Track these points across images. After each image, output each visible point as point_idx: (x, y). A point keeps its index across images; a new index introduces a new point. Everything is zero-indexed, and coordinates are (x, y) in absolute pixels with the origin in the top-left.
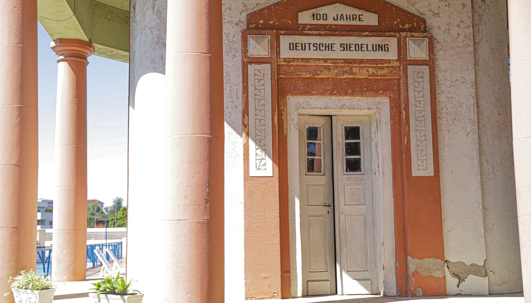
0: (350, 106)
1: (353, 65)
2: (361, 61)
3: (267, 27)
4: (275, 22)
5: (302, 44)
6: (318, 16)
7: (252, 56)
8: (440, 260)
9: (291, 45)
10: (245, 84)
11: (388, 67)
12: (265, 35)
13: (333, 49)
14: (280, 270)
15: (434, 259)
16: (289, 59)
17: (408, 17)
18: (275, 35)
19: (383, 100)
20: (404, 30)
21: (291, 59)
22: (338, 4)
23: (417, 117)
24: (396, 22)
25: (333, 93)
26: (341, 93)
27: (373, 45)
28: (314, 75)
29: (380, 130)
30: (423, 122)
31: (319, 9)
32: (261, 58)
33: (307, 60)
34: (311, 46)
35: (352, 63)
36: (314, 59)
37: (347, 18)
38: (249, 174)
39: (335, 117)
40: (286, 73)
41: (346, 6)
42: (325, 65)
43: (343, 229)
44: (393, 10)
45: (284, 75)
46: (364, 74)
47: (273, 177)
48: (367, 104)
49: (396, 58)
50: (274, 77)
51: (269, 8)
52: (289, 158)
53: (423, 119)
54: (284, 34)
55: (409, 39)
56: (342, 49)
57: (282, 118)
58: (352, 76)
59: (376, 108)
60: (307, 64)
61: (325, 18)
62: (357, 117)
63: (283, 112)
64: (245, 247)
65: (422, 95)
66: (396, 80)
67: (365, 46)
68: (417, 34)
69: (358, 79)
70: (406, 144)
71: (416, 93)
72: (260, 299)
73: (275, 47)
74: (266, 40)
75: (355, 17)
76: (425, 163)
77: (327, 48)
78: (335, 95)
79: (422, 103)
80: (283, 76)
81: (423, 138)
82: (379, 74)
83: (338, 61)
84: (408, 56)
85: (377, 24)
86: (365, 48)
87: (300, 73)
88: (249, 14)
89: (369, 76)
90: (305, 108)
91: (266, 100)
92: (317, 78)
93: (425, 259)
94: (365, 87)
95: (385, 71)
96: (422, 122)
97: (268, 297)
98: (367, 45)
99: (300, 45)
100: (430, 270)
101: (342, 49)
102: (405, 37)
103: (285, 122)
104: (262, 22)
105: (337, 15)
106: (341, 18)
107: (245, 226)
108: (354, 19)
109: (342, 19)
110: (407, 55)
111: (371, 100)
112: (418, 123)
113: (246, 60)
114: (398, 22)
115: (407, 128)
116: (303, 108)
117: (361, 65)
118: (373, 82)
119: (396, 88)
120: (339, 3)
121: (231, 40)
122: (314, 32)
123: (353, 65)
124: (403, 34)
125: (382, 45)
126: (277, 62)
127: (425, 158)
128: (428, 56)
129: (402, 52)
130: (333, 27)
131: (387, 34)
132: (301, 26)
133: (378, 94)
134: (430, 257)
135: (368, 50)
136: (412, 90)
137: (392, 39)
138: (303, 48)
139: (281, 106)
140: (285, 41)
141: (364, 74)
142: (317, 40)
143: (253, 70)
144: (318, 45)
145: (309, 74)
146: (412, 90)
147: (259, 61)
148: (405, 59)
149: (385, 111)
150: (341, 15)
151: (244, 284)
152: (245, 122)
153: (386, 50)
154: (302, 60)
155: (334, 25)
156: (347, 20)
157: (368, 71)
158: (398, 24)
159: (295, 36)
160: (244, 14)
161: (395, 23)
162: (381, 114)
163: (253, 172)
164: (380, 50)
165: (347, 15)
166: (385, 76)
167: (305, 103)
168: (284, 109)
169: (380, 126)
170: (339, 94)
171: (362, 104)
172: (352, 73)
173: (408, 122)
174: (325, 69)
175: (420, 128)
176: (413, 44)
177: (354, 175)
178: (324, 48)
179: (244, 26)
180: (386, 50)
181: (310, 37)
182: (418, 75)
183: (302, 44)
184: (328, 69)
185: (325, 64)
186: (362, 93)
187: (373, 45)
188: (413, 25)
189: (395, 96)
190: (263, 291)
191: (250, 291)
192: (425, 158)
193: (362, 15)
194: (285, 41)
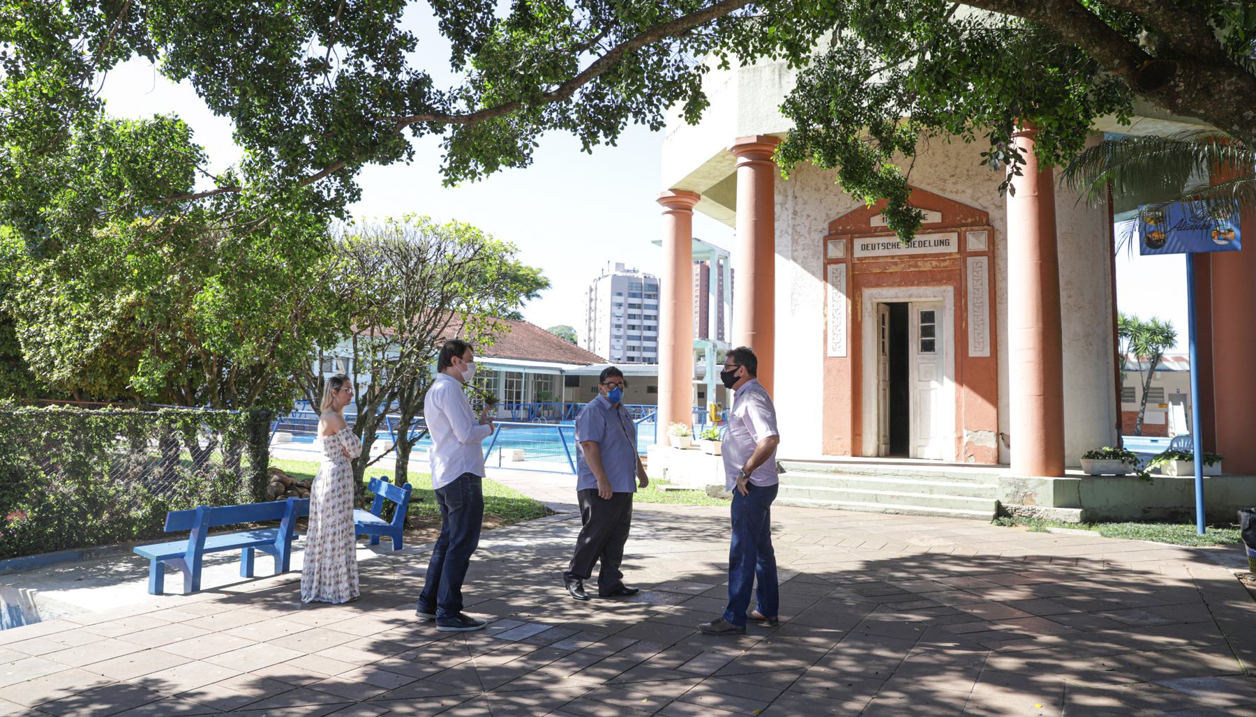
2: (925, 256)
3: (844, 233)
20: (966, 225)
33: (877, 258)
51: (846, 216)
52: (863, 341)
68: (977, 228)
73: (850, 248)
85: (940, 221)
86: (927, 244)
95: (947, 263)
102: (966, 231)
112: (976, 309)
119: (958, 277)
124: (964, 229)
138: (873, 248)
140: (858, 243)
142: (885, 240)
147: (836, 261)
148: (965, 251)
154: (873, 258)
163: (831, 353)
170: (906, 285)
172: (917, 266)
173: (966, 309)
177: (928, 354)
179: (826, 233)
184: (896, 264)
186: (927, 283)
194: (858, 243)
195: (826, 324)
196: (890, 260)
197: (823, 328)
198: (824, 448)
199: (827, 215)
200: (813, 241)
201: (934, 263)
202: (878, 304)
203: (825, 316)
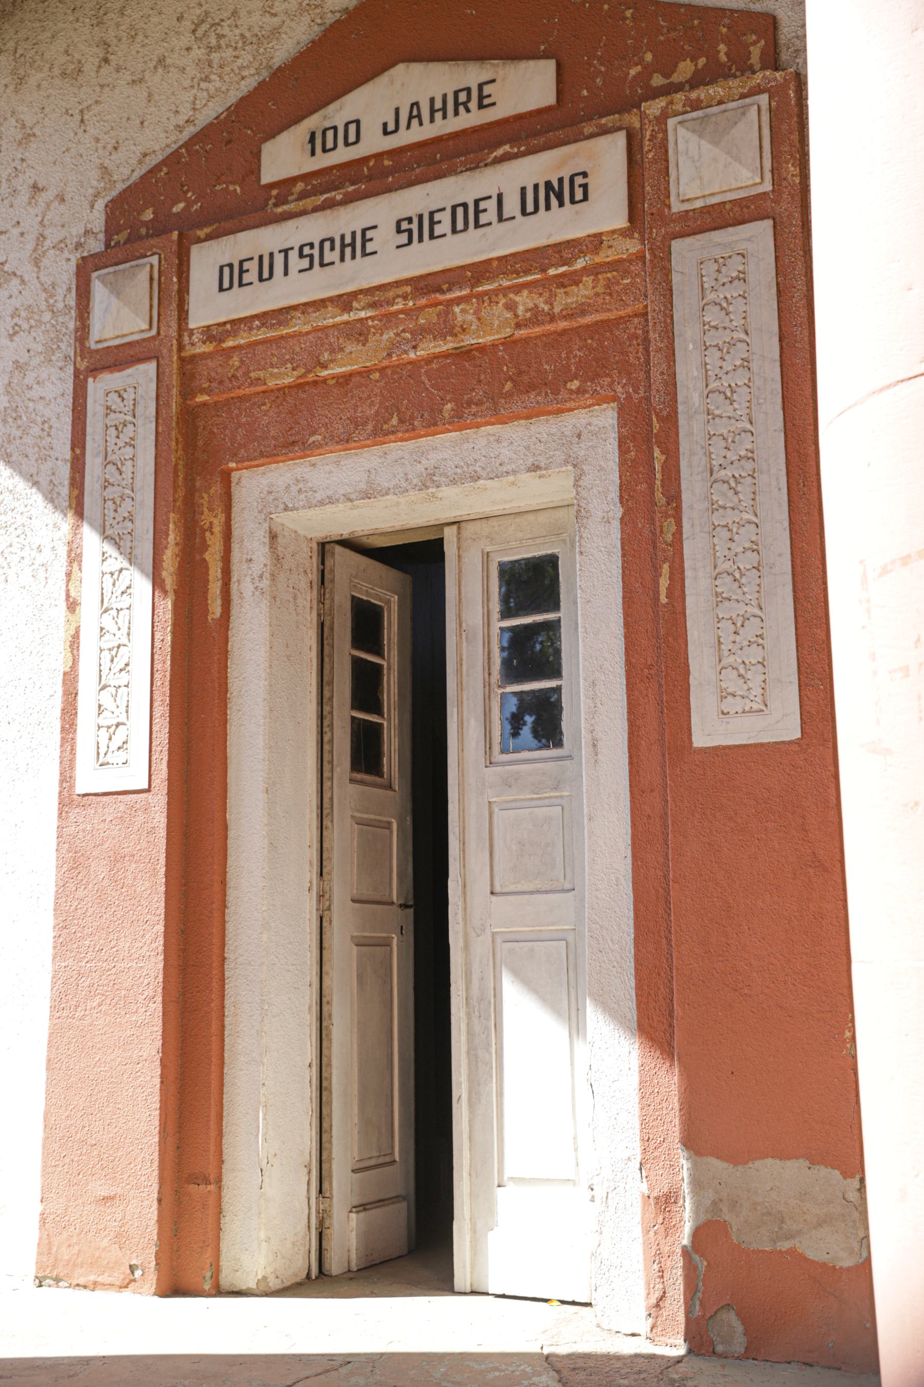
0: (459, 471)
1: (449, 296)
3: (159, 229)
4: (189, 204)
5: (261, 257)
6: (330, 134)
7: (100, 346)
8: (837, 1173)
9: (226, 271)
10: (78, 451)
11: (594, 270)
12: (146, 256)
13: (370, 247)
14: (156, 1173)
15: (803, 1163)
16: (221, 329)
17: (692, 28)
18: (175, 248)
19: (595, 421)
21: (228, 327)
22: (401, 67)
23: (716, 468)
24: (639, 68)
25: (385, 427)
26: (416, 423)
27: (523, 190)
28: (309, 371)
29: (581, 553)
30: (745, 489)
31: (332, 107)
32: (130, 344)
33: (281, 315)
34: (293, 255)
35: (445, 287)
36: (304, 307)
37: (433, 111)
38: (72, 786)
39: (455, 527)
40: (214, 385)
41: (432, 65)
42: (347, 323)
43: (481, 1000)
44: (625, 18)
45: (208, 391)
46: (496, 323)
47: (148, 790)
48: (528, 448)
49: (622, 222)
50: (168, 405)
53: (743, 469)
54: (209, 238)
55: (680, 123)
56: (404, 238)
57: (205, 560)
58: (447, 345)
59: (566, 462)
60: (285, 331)
61: (352, 138)
62: (542, 517)
63: (208, 534)
64: (48, 1069)
65: (738, 363)
66: (636, 320)
67: (491, 206)
68: (716, 90)
69: (482, 349)
70: (663, 599)
71: (713, 357)
72: (85, 1287)
74: (143, 275)
75: (463, 97)
76: (755, 680)
77: (348, 250)
78: (393, 433)
79: (742, 396)
80: (205, 398)
81: (746, 561)
82: (557, 310)
83: (391, 294)
84: (673, 198)
86: (490, 215)
87: (261, 374)
88: (111, 201)
89: (518, 326)
90: (294, 509)
91: (138, 497)
92: (325, 381)
93: (758, 1163)
94: (510, 378)
96: (739, 488)
97: (109, 1280)
98: (500, 197)
99: (253, 266)
100: (783, 1222)
101: (404, 238)
102: (662, 119)
103: (215, 572)
104: (148, 215)
105: (397, 111)
106: (411, 117)
107: (54, 984)
108: (461, 108)
109: (415, 122)
110: (669, 197)
111: (544, 427)
113: (83, 365)
114: (645, 68)
115: (670, 526)
116: (286, 509)
117: (480, 289)
118: (540, 350)
120: (403, 61)
121: (60, 305)
122: (309, 203)
123: (449, 296)
124: (654, 108)
125: (561, 180)
126: (181, 348)
127: (754, 656)
128: (768, 176)
129: (648, 188)
130: (387, 163)
131: (588, 129)
132: (274, 192)
133: (563, 394)
134: (783, 1155)
135: (505, 216)
136: (691, 346)
137: (603, 142)
139: (202, 513)
141: (496, 323)
143: (101, 393)
144: (317, 246)
145: (294, 369)
146: (691, 346)
148: (662, 216)
149: (601, 469)
150: (412, 105)
151: (37, 1218)
152: (72, 594)
153: (579, 195)
154: (263, 317)
155: (391, 153)
156: (432, 120)
157: (511, 307)
158: (648, 71)
159: (239, 235)
160: (100, 204)
161: (633, 72)
162: (586, 481)
164: (554, 202)
165: (432, 100)
166: (583, 313)
167: (294, 489)
168: (211, 523)
169: (581, 537)
171: (506, 453)
172: (448, 330)
173: (674, 499)
174: (348, 337)
175: (730, 517)
176: (694, 138)
178: (334, 256)
179: (96, 245)
180: (579, 195)
181: (291, 224)
182: (719, 271)
183: (261, 257)
185: (345, 317)
187: (523, 190)
188: (712, 56)
189: (636, 392)
190: (97, 1254)
191: (54, 1249)
192: (754, 656)
193: (493, 81)
195: (74, 642)
196: (334, 318)
197: (59, 662)
198: (46, 1247)
199: (105, 170)
200: (49, 291)
201: (524, 301)
202: (323, 548)
203: (72, 606)
